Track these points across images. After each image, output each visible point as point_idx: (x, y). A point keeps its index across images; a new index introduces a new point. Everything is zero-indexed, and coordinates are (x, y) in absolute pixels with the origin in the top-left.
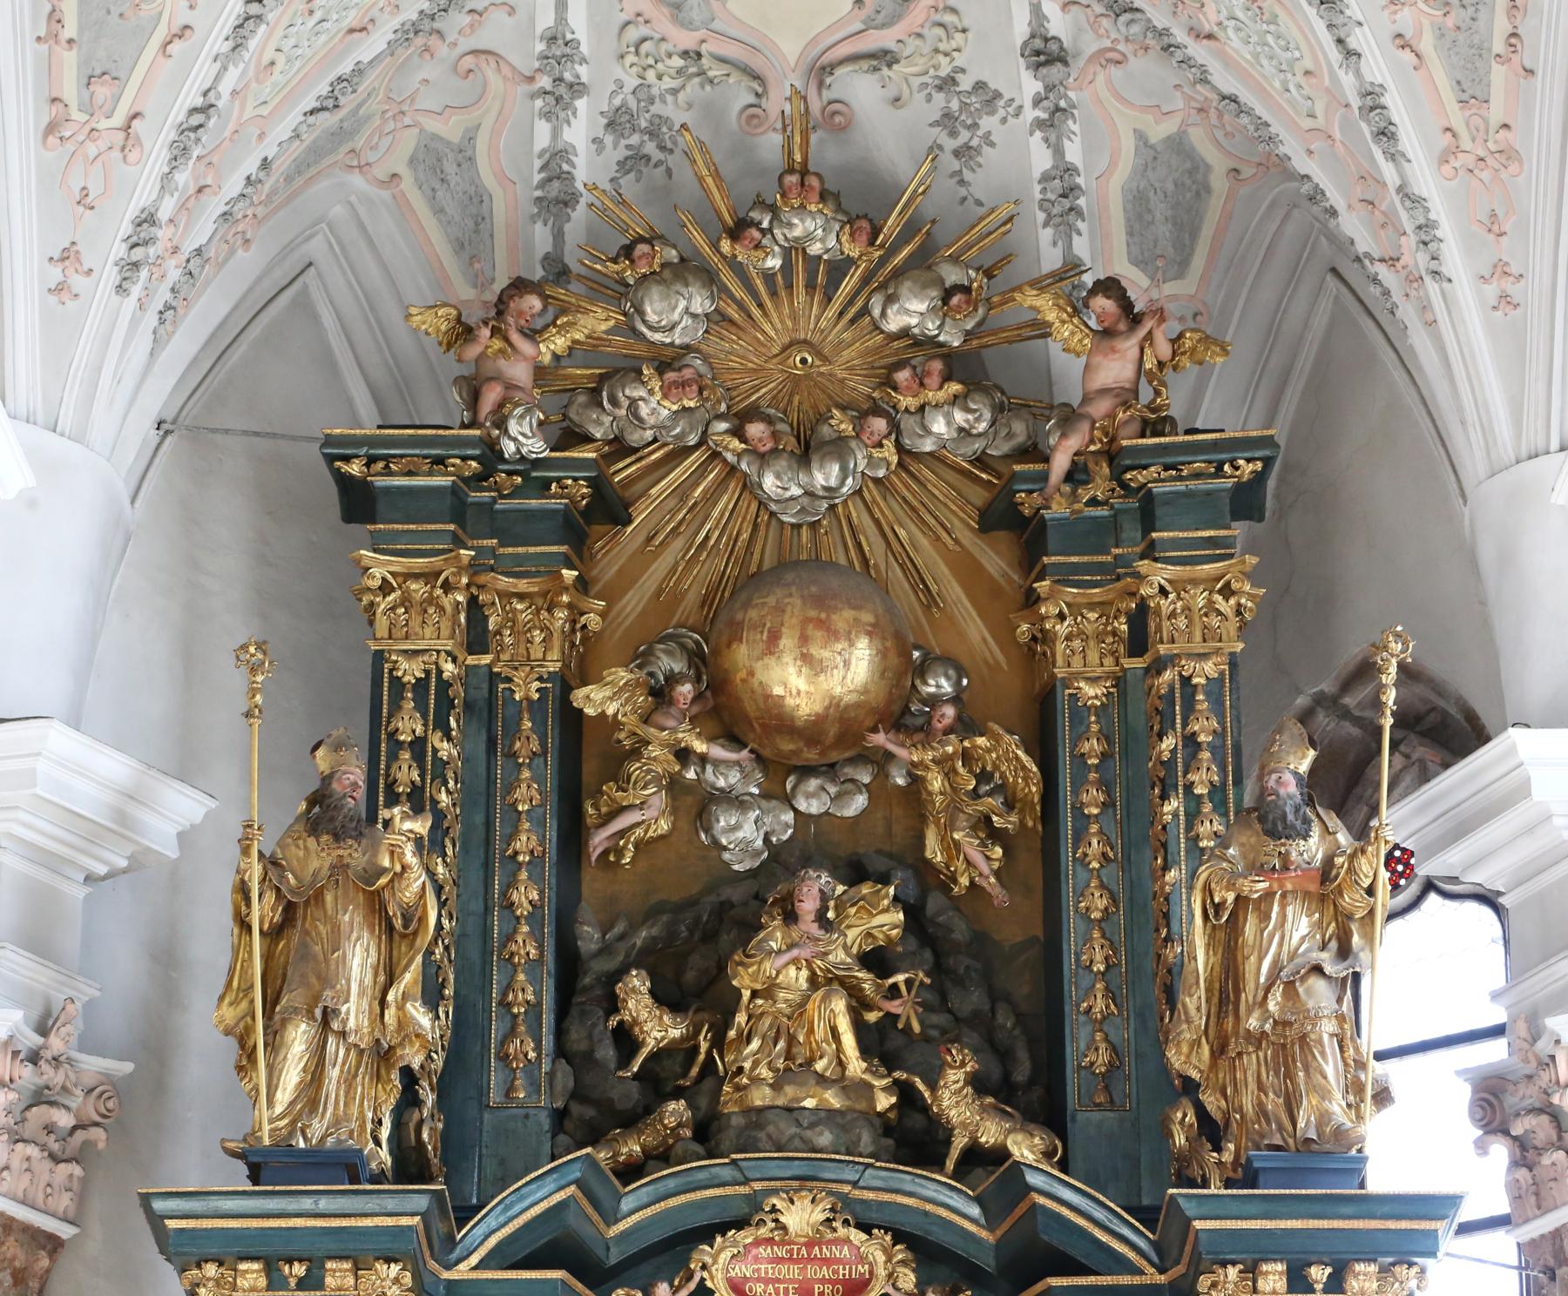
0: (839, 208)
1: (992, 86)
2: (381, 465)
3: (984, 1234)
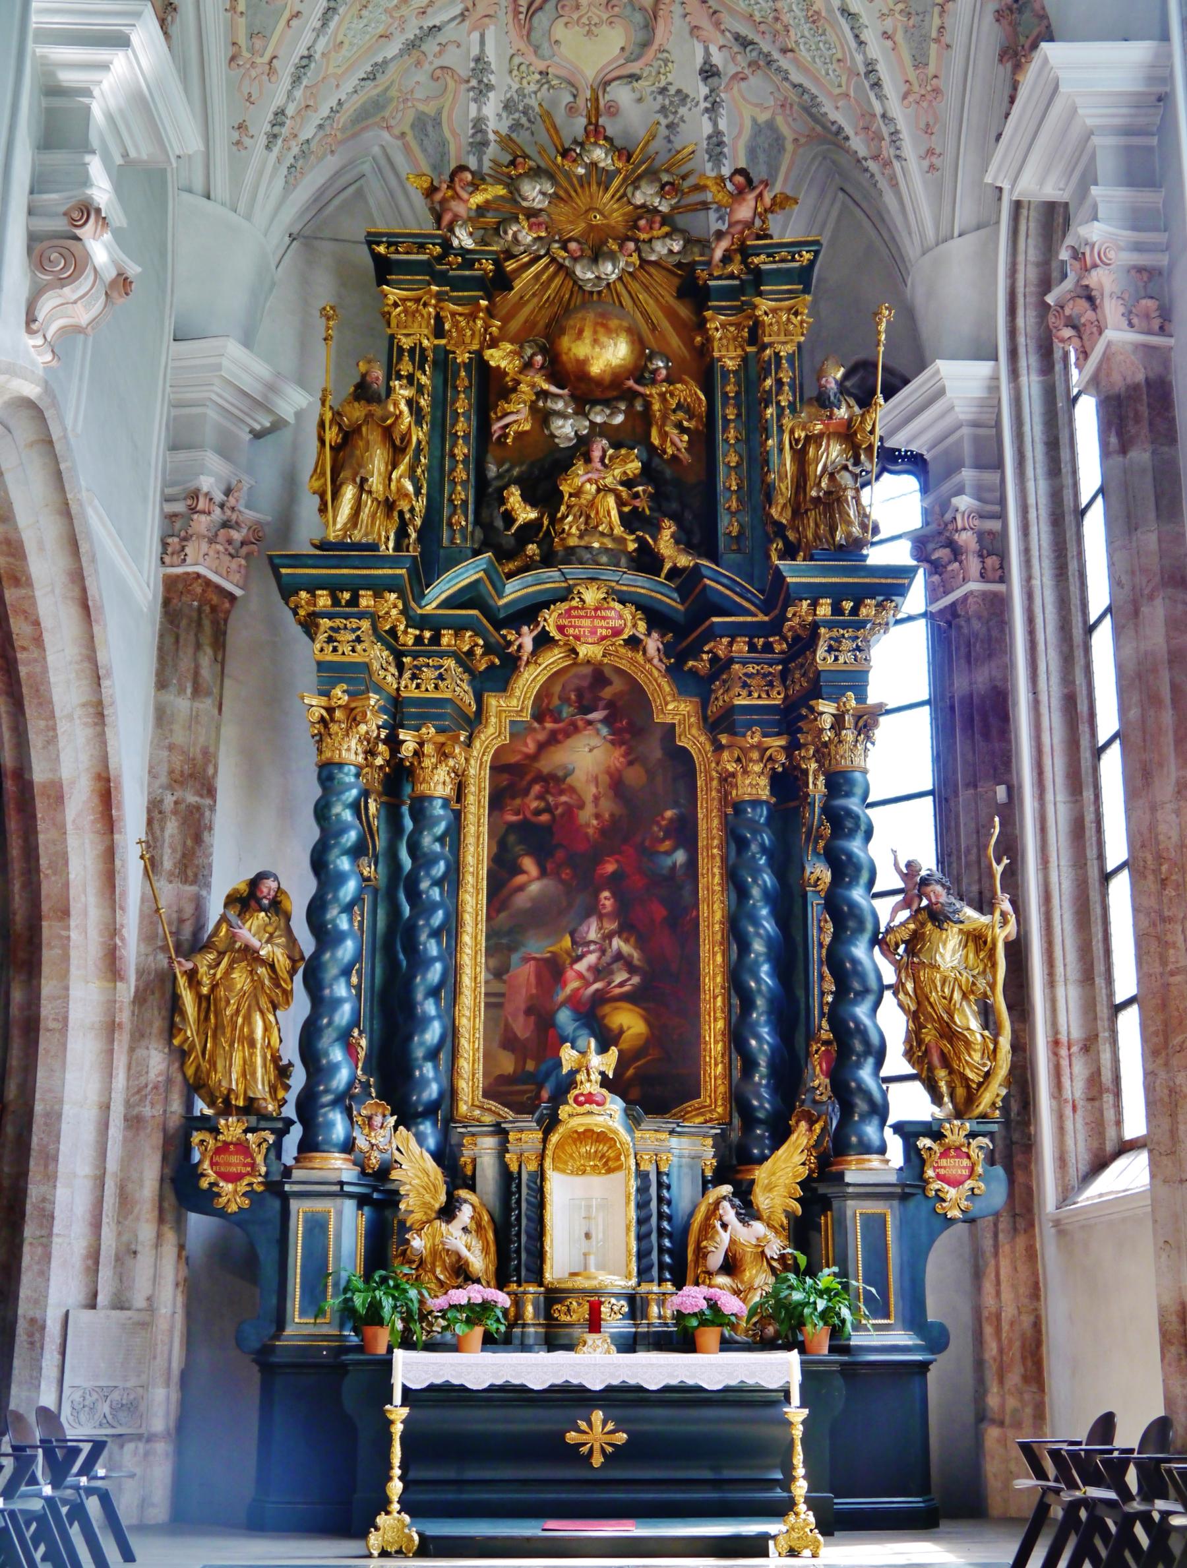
2: (392, 249)
3: (680, 607)
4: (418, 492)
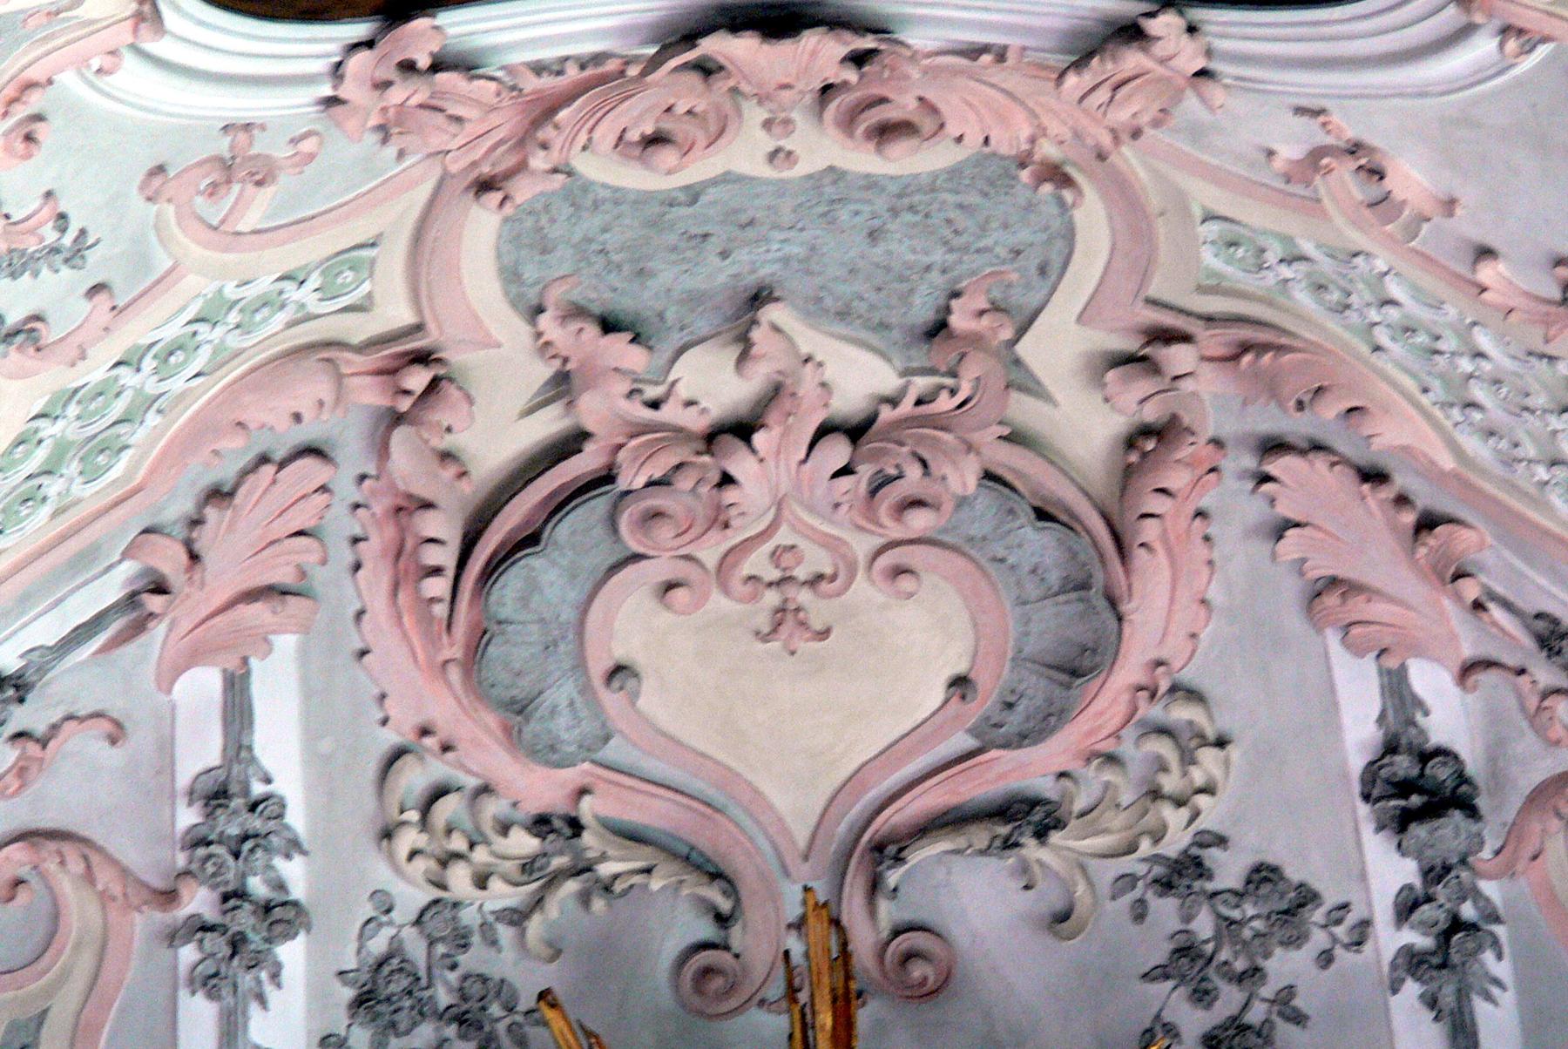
1: (1294, 874)
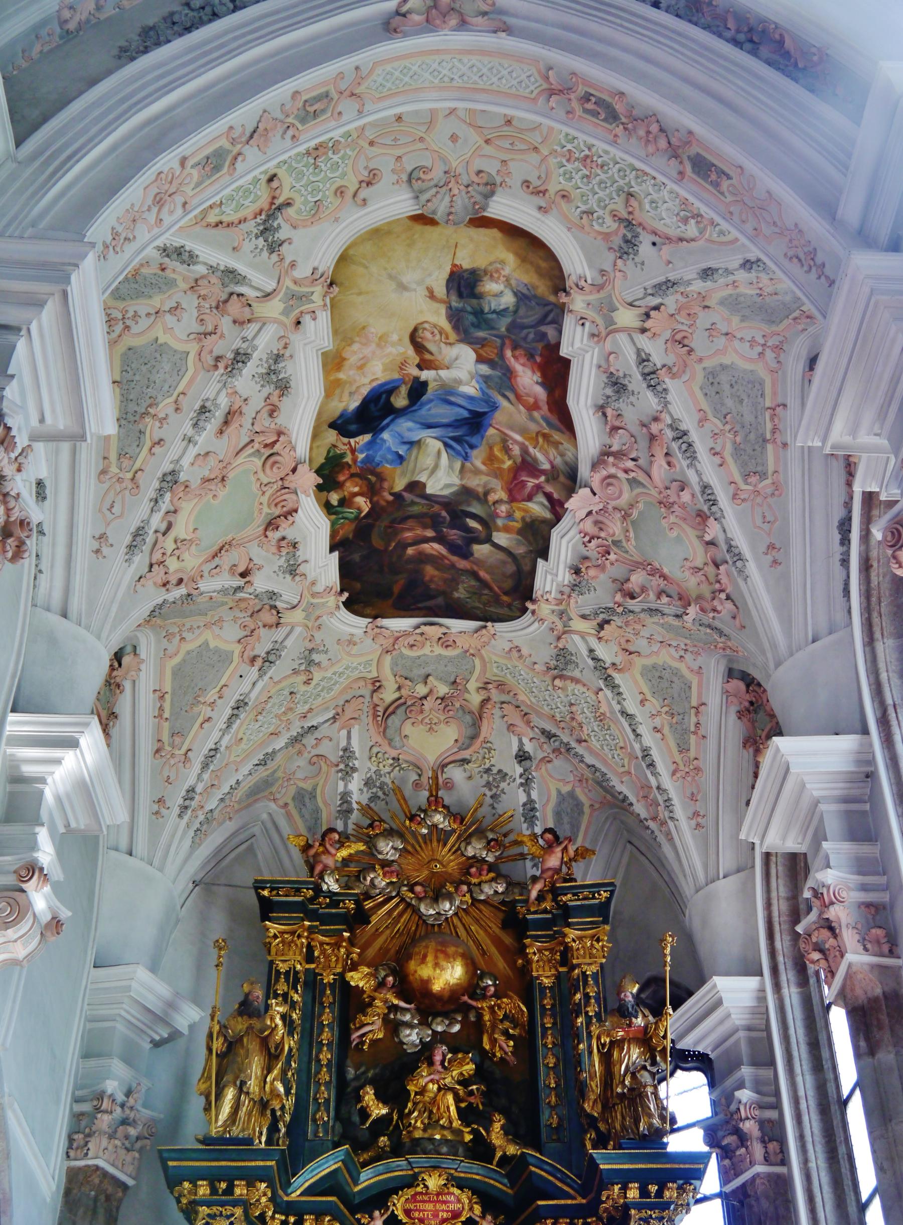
0: (449, 811)
2: (274, 892)
3: (509, 1191)
4: (288, 1092)
